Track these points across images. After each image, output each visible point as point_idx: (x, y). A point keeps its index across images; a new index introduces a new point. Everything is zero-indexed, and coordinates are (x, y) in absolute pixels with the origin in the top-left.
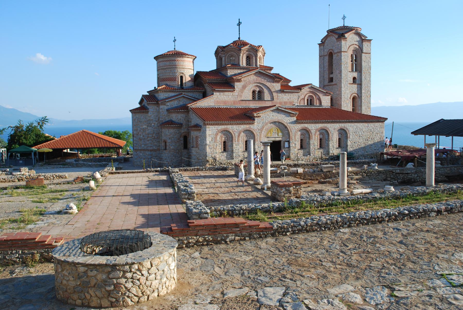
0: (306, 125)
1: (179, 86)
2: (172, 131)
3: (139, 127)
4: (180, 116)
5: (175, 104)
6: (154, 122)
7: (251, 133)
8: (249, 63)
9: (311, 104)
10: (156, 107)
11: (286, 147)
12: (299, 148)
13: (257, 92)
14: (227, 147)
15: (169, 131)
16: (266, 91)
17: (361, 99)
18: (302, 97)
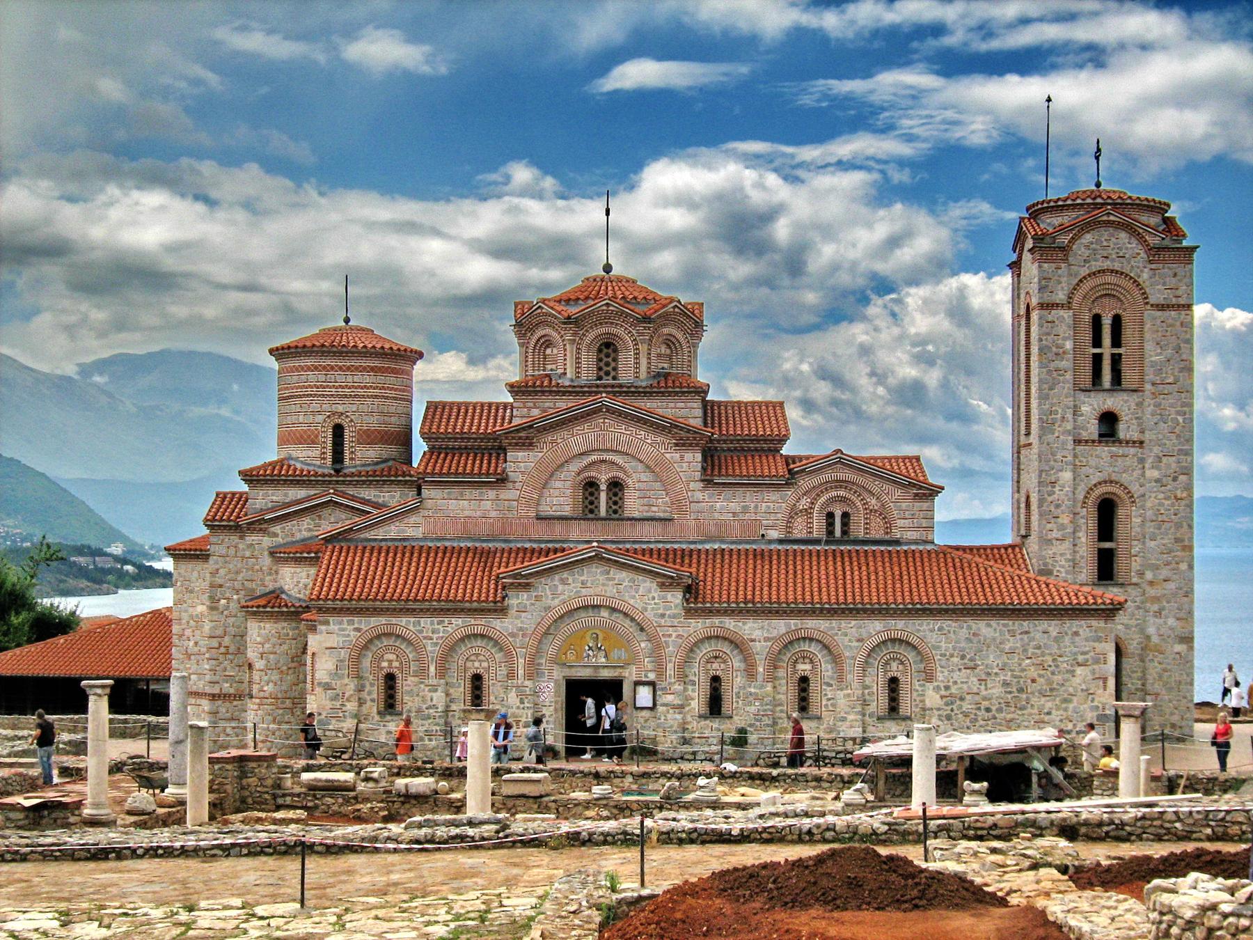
0: (730, 623)
1: (329, 461)
2: (269, 627)
3: (186, 611)
4: (304, 574)
5: (303, 529)
6: (227, 595)
7: (495, 646)
8: (615, 369)
9: (844, 532)
10: (234, 539)
11: (638, 705)
12: (705, 710)
13: (603, 487)
14: (398, 696)
15: (260, 628)
16: (636, 479)
17: (1143, 507)
18: (804, 503)
